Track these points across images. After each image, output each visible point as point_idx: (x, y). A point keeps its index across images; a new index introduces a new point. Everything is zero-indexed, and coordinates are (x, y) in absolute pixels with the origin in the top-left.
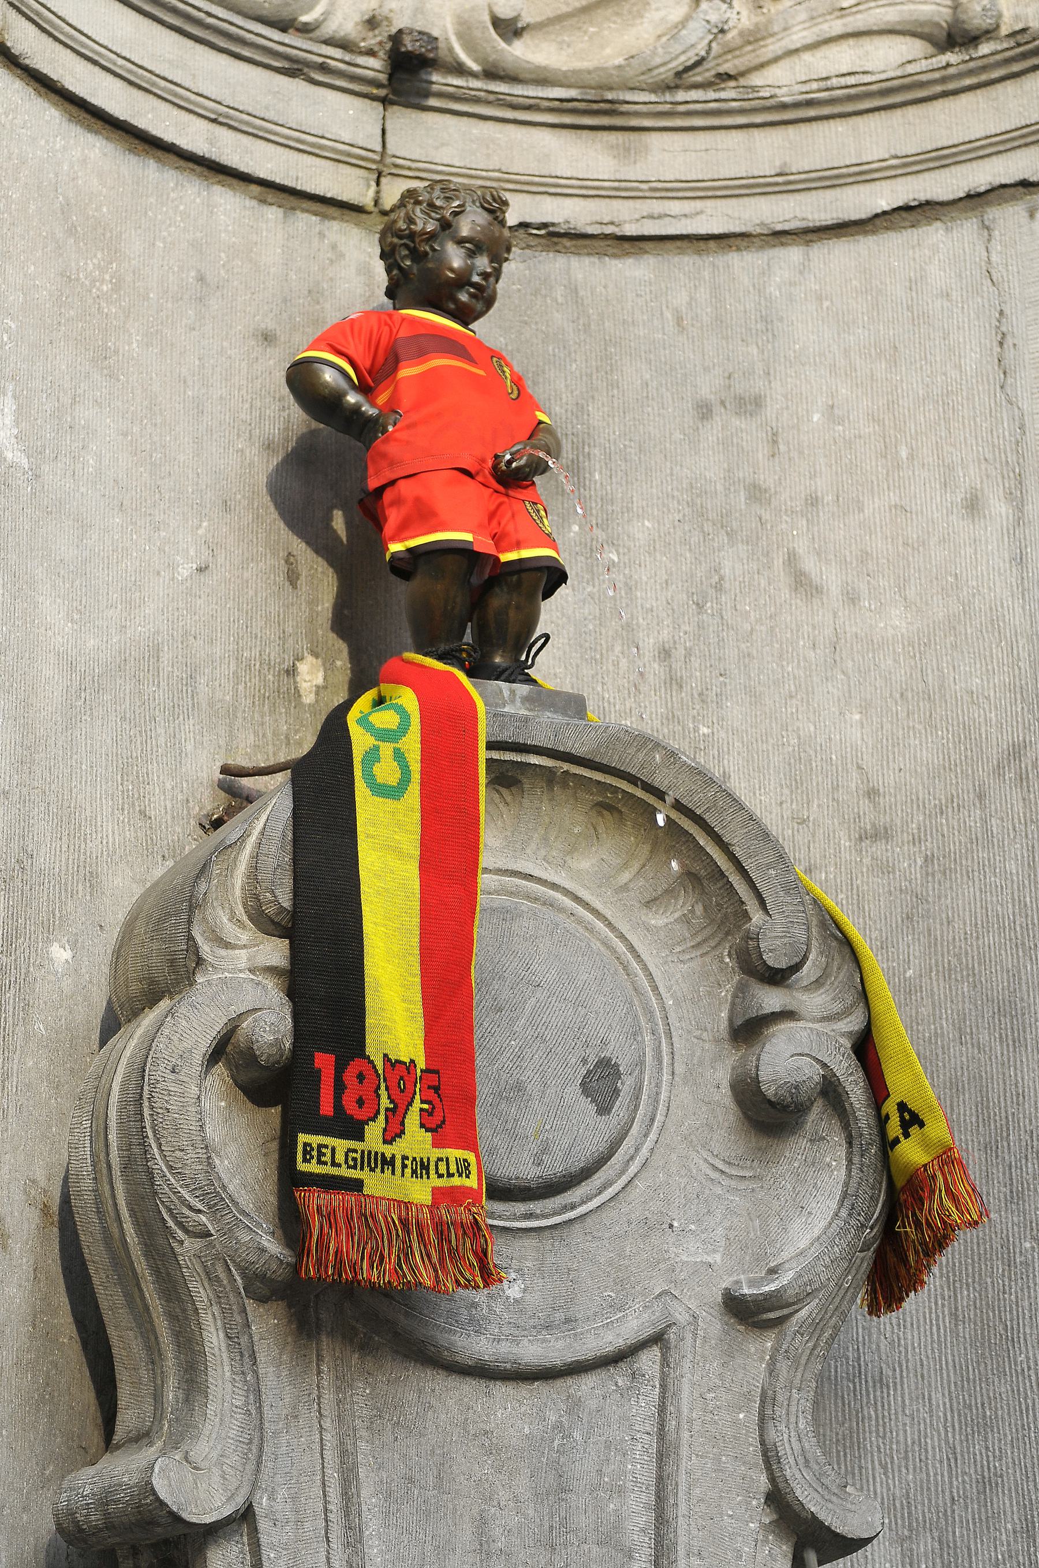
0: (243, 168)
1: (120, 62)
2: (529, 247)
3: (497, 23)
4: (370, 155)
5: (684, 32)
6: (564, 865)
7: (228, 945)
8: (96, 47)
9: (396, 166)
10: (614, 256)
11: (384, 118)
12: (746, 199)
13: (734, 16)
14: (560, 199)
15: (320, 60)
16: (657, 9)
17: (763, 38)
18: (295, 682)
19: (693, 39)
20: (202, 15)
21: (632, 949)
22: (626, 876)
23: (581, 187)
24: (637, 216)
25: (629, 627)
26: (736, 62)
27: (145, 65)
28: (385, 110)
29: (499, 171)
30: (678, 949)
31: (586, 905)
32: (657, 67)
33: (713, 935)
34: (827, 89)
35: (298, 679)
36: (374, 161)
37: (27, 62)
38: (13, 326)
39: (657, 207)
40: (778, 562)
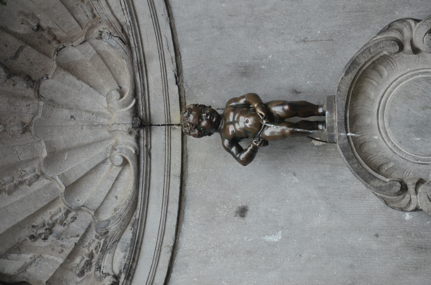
0: (180, 166)
1: (164, 208)
2: (182, 81)
3: (122, 97)
4: (167, 129)
5: (113, 45)
6: (373, 100)
7: (411, 200)
8: (162, 216)
9: (168, 121)
10: (181, 58)
11: (155, 125)
12: (160, 24)
13: (105, 30)
14: (168, 74)
15: (145, 147)
16: (104, 48)
17: (110, 21)
18: (320, 146)
19: (114, 42)
20: (144, 185)
21: (395, 81)
22: (374, 83)
23: (163, 69)
24: (169, 52)
25: (291, 52)
26: (118, 28)
27: (162, 200)
28: (153, 125)
29: (163, 92)
30: (393, 67)
31: (384, 94)
32: (124, 50)
33: (389, 60)
34: (126, 9)
35: (319, 145)
36: (168, 128)
37: (174, 237)
38: (245, 238)
39: (165, 47)
40: (268, 14)
